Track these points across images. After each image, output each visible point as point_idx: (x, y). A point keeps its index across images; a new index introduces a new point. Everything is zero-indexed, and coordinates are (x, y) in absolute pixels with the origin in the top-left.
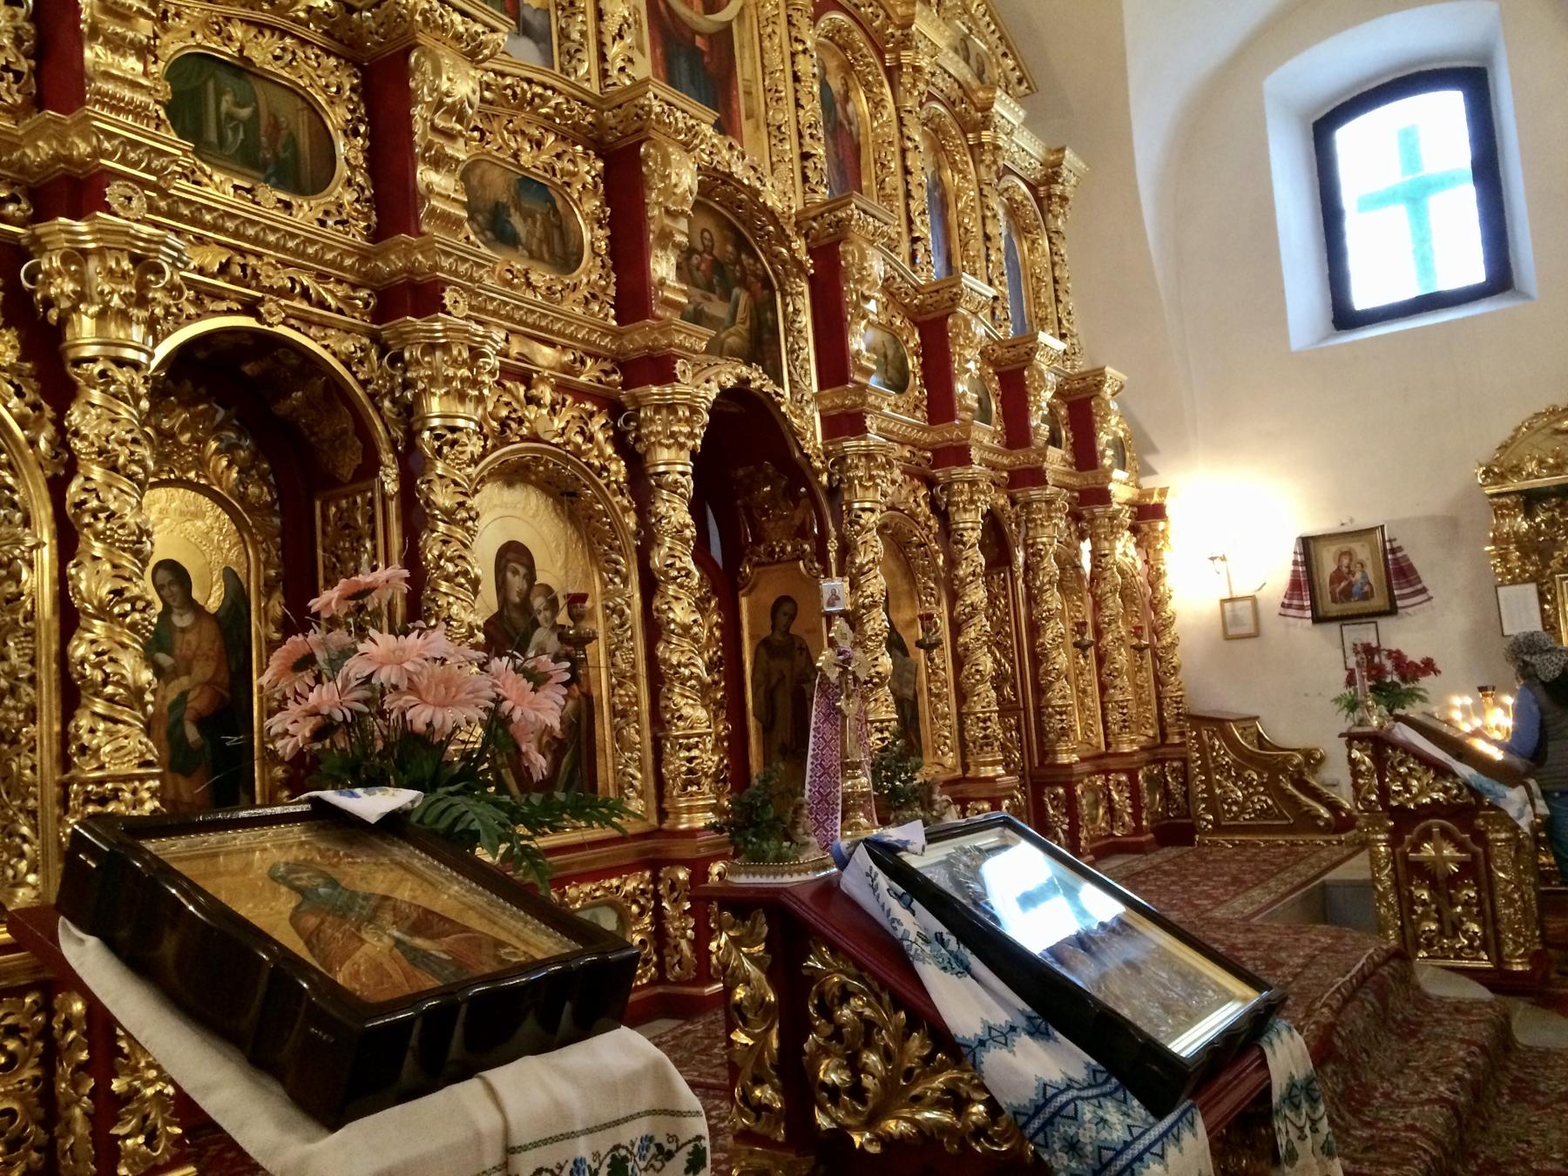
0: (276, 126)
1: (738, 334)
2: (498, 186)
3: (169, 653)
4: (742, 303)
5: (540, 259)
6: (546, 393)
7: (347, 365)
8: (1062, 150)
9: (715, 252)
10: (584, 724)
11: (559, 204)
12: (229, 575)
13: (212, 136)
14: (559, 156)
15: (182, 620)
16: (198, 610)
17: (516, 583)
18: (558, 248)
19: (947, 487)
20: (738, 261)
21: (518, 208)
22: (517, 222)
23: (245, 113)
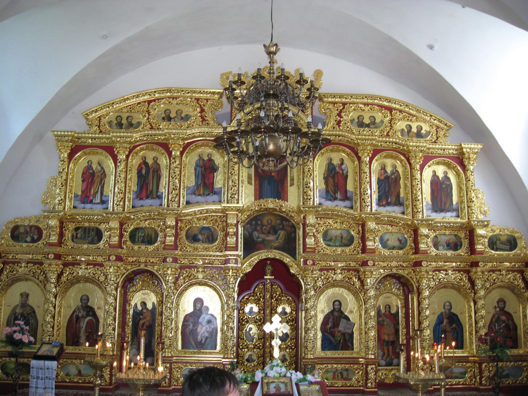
0: (148, 235)
1: (279, 242)
2: (196, 231)
3: (142, 315)
4: (281, 234)
5: (206, 242)
6: (200, 270)
7: (157, 271)
8: (461, 145)
9: (273, 224)
10: (214, 333)
11: (212, 230)
12: (153, 303)
13: (137, 240)
14: (212, 220)
15: (145, 311)
16: (147, 309)
17: (199, 305)
18: (211, 239)
19: (364, 272)
20: (282, 224)
21: (200, 233)
22: (200, 237)
23: (143, 234)
